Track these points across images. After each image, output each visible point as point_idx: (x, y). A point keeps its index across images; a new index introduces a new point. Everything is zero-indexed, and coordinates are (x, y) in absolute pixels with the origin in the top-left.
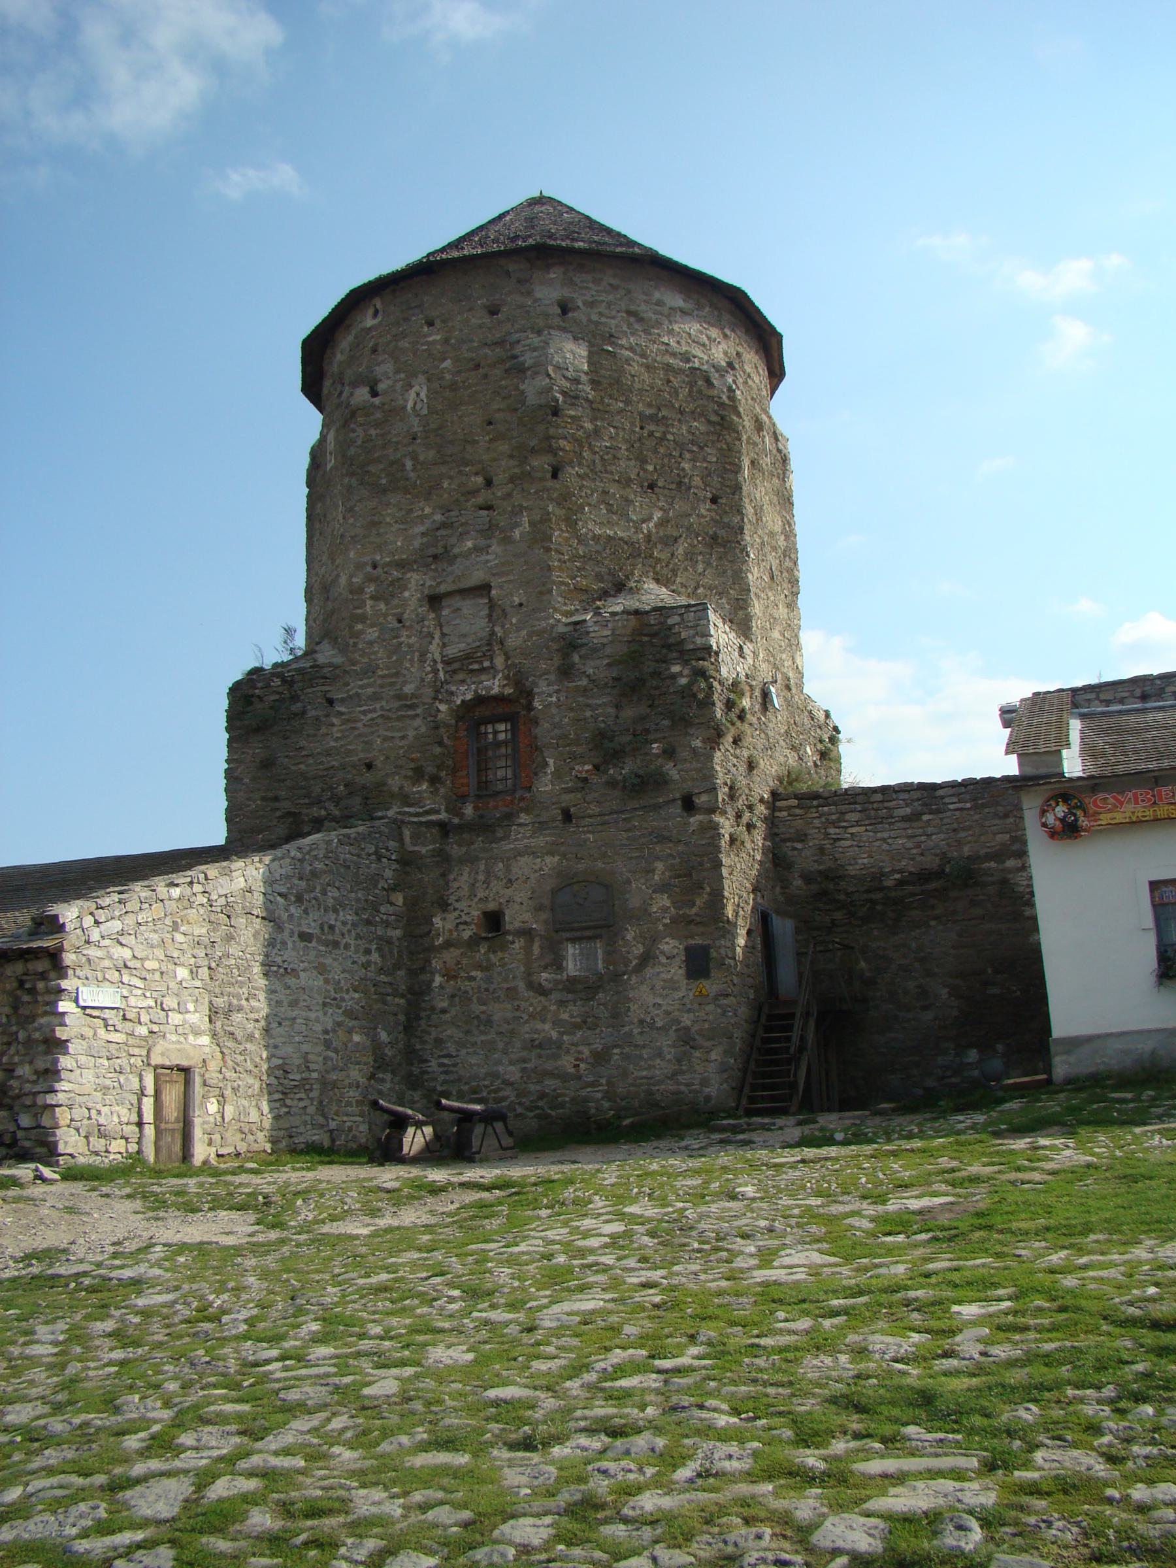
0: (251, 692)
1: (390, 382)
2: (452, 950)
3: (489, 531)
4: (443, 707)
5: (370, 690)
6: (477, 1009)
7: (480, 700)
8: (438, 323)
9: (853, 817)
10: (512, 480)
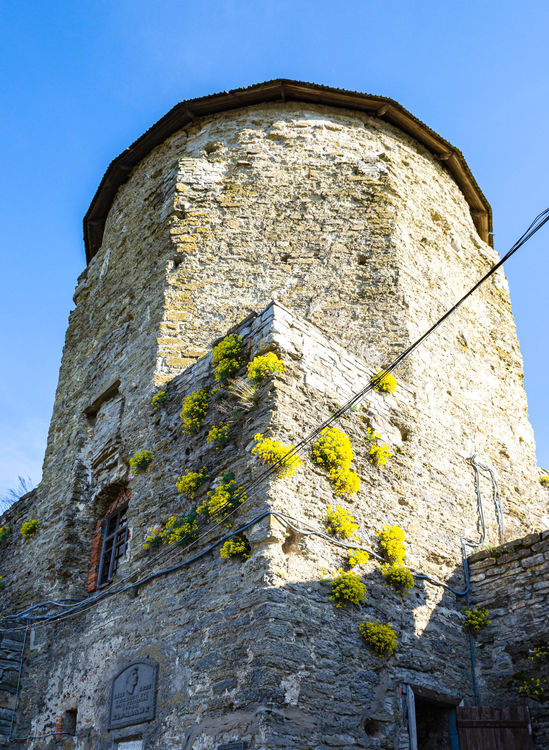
4: (81, 507)
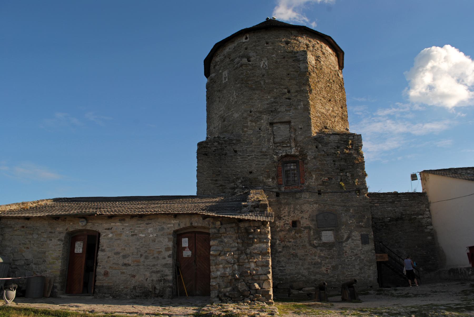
0: (206, 146)
1: (255, 58)
2: (283, 232)
3: (290, 105)
4: (275, 157)
5: (250, 149)
6: (293, 252)
7: (287, 156)
8: (270, 44)
9: (376, 201)
10: (297, 91)
